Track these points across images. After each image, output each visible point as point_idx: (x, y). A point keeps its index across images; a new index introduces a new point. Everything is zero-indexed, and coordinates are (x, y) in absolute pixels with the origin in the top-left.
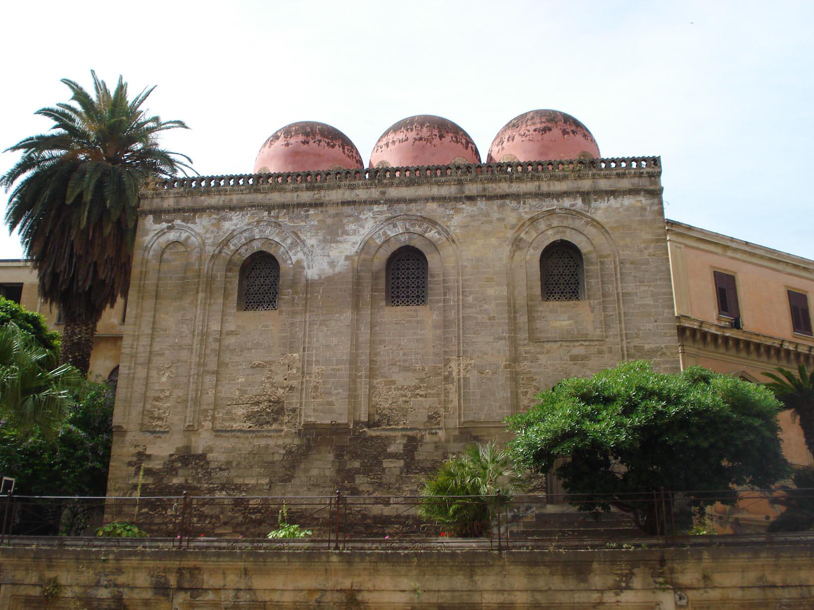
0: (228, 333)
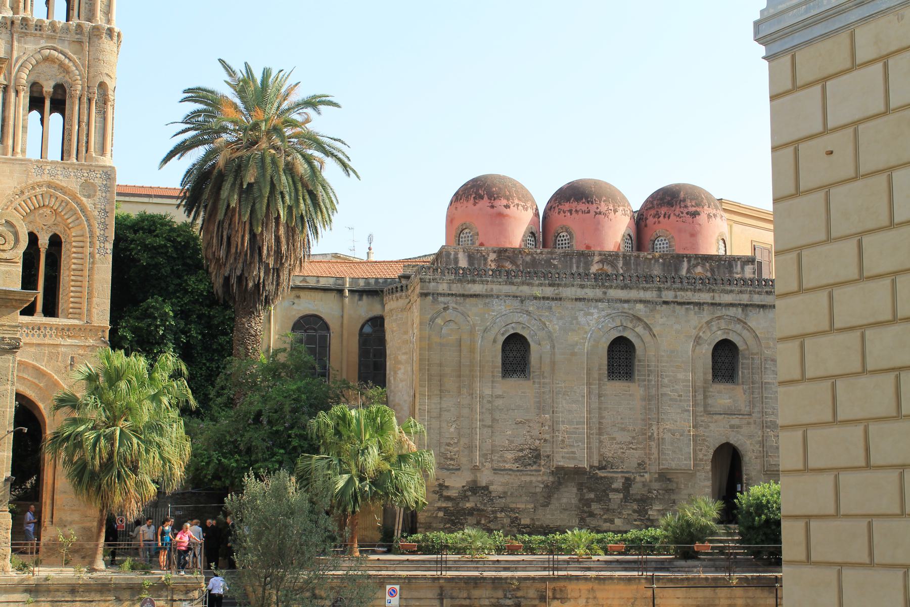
0: (498, 397)
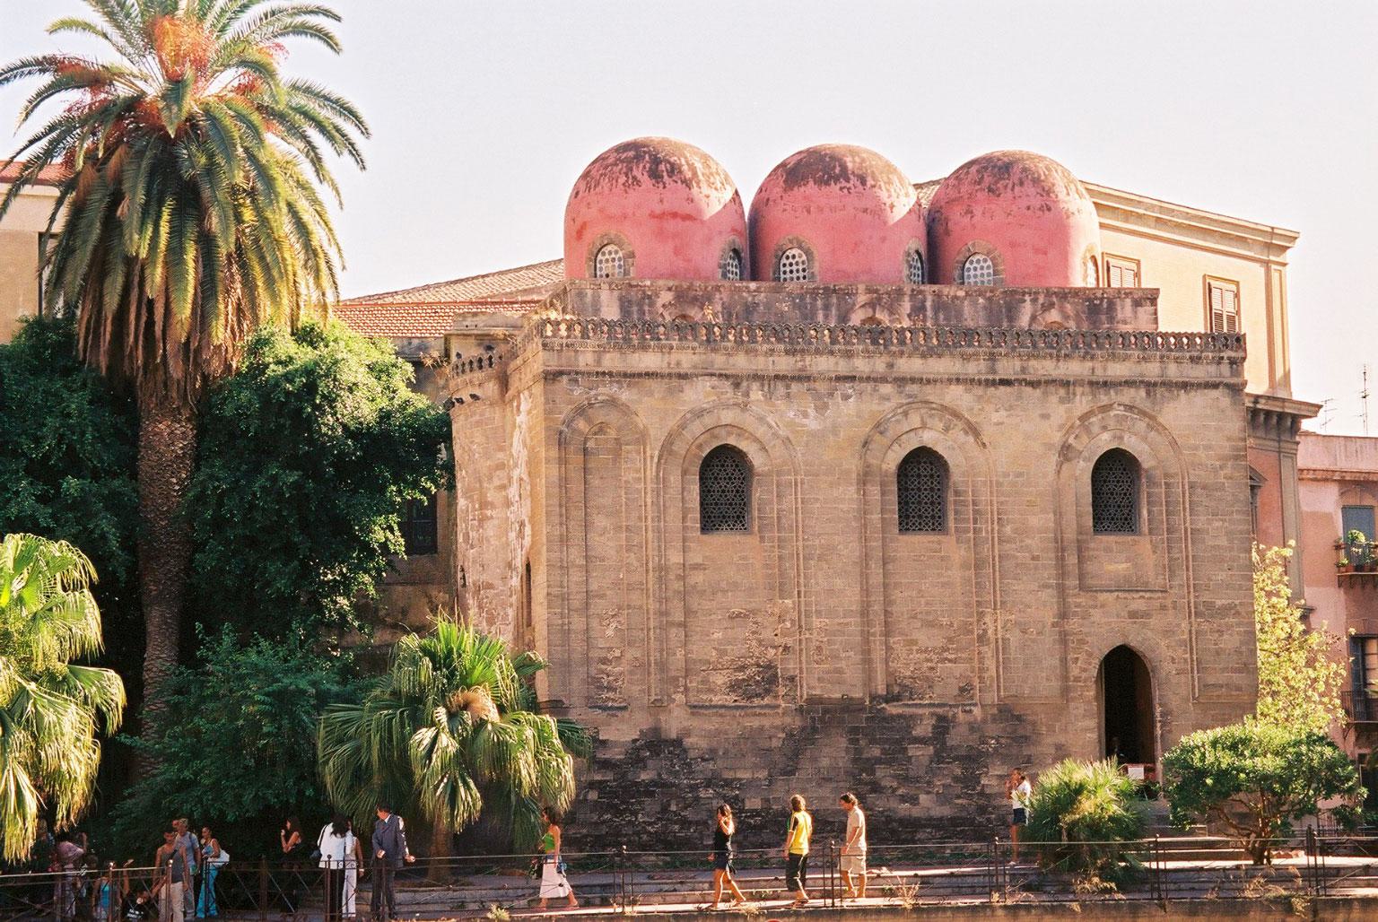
0: (696, 567)
